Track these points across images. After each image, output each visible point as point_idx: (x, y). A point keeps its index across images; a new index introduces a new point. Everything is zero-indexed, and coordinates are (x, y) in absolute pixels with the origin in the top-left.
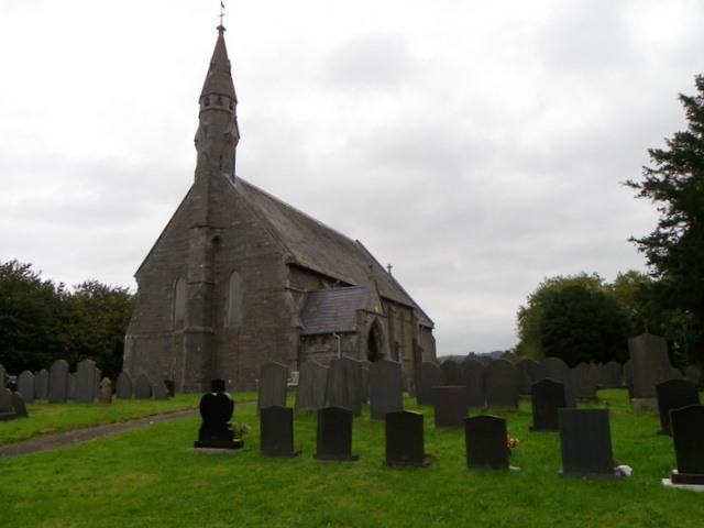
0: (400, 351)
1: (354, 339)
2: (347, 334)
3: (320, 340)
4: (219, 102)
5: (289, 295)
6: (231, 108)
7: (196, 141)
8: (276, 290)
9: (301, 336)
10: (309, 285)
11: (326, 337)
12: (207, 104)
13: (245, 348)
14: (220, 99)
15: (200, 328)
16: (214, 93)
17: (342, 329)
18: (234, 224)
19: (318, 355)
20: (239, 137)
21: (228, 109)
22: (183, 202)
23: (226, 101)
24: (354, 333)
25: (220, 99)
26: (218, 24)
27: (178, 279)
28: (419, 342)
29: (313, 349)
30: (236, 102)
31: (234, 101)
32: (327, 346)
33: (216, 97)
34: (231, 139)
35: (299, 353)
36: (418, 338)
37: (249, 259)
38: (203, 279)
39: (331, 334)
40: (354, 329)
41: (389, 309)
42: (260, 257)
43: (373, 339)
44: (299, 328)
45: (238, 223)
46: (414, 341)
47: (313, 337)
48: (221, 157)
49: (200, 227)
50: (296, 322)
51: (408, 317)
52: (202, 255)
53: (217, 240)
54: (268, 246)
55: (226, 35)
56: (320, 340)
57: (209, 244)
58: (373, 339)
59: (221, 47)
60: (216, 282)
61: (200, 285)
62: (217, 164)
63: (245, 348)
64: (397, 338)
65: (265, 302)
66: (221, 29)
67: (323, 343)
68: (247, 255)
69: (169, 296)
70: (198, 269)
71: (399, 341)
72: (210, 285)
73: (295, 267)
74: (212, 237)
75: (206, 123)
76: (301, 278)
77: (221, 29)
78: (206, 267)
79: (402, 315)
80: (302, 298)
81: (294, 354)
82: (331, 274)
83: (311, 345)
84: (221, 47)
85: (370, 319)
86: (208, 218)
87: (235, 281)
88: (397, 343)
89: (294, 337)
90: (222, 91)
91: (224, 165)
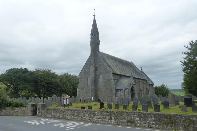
0: (142, 92)
1: (127, 90)
2: (126, 89)
3: (120, 90)
4: (95, 35)
5: (113, 80)
10: (117, 77)
11: (121, 90)
12: (92, 36)
13: (104, 92)
15: (94, 88)
16: (94, 33)
23: (96, 34)
24: (127, 89)
28: (148, 89)
29: (118, 92)
32: (122, 92)
34: (98, 44)
35: (115, 93)
36: (148, 88)
40: (127, 88)
41: (139, 81)
43: (132, 90)
44: (115, 88)
46: (147, 89)
47: (118, 90)
49: (92, 65)
50: (114, 87)
51: (145, 82)
52: (93, 71)
53: (96, 68)
56: (120, 90)
58: (132, 90)
60: (97, 77)
62: (95, 50)
63: (104, 92)
64: (141, 88)
66: (94, 16)
68: (103, 71)
70: (92, 74)
71: (142, 89)
72: (95, 78)
73: (114, 74)
75: (92, 40)
76: (115, 76)
77: (94, 16)
79: (143, 82)
80: (116, 80)
82: (123, 74)
83: (118, 91)
85: (131, 86)
86: (94, 63)
87: (101, 76)
88: (141, 90)
89: (114, 90)
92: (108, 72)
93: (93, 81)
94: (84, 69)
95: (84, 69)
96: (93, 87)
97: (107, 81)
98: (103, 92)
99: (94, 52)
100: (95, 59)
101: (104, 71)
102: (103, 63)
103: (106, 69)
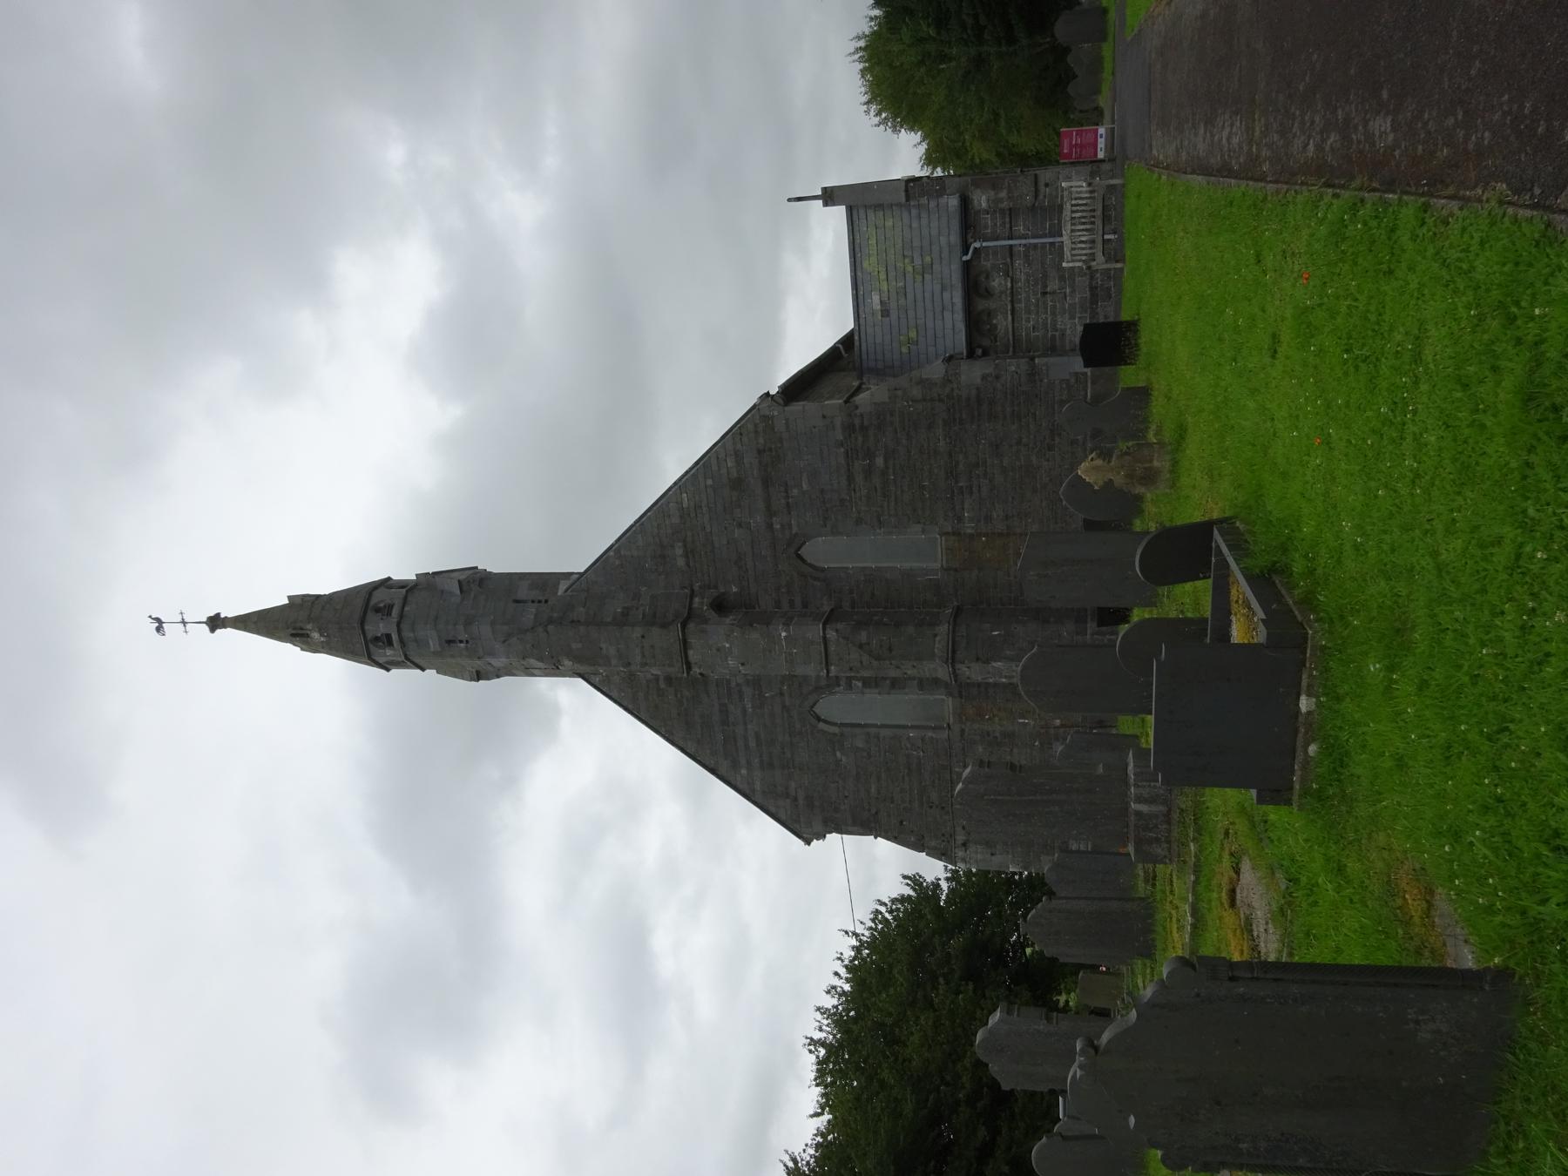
3: (982, 304)
4: (385, 611)
6: (403, 587)
7: (478, 676)
8: (849, 429)
9: (971, 354)
11: (973, 284)
14: (377, 610)
15: (943, 629)
16: (362, 623)
17: (955, 238)
18: (681, 562)
19: (1021, 306)
20: (476, 568)
21: (404, 590)
22: (626, 709)
24: (965, 202)
25: (377, 610)
26: (205, 628)
27: (819, 719)
29: (1003, 323)
30: (389, 579)
31: (386, 583)
32: (997, 283)
33: (371, 616)
37: (770, 512)
38: (814, 631)
39: (967, 267)
40: (953, 202)
42: (766, 482)
45: (679, 551)
47: (975, 322)
48: (517, 601)
49: (685, 644)
53: (721, 606)
55: (228, 612)
56: (982, 304)
57: (728, 621)
59: (262, 623)
61: (831, 634)
62: (532, 609)
65: (880, 461)
66: (215, 623)
67: (988, 294)
69: (860, 744)
74: (712, 614)
77: (215, 623)
78: (787, 625)
81: (1014, 367)
84: (262, 623)
86: (664, 626)
87: (824, 551)
89: (973, 373)
93: (863, 636)
94: (735, 765)
95: (735, 765)
96: (939, 645)
97: (868, 472)
99: (551, 621)
100: (626, 613)
102: (676, 520)
103: (737, 484)
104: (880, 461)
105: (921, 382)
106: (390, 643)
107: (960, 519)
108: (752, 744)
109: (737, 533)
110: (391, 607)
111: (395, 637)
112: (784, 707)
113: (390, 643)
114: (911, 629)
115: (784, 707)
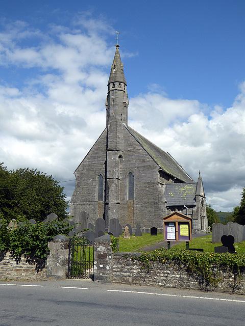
14: (120, 84)
17: (188, 204)
18: (129, 149)
24: (195, 206)
37: (138, 167)
42: (144, 167)
45: (131, 149)
54: (149, 161)
65: (148, 189)
90: (122, 81)
91: (123, 118)
92: (150, 168)
97: (145, 187)
98: (135, 212)
101: (140, 165)
103: (144, 161)
104: (148, 189)
105: (162, 197)
106: (113, 87)
107: (136, 204)
108: (94, 162)
109: (135, 161)
110: (120, 87)
111: (114, 88)
112: (101, 169)
113: (113, 87)
114: (115, 195)
115: (101, 169)
